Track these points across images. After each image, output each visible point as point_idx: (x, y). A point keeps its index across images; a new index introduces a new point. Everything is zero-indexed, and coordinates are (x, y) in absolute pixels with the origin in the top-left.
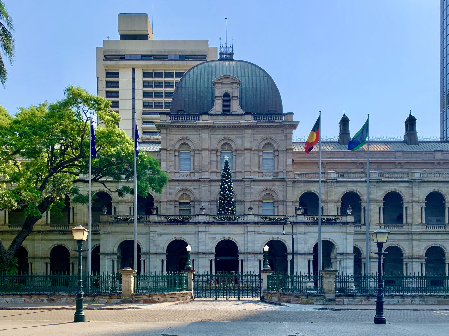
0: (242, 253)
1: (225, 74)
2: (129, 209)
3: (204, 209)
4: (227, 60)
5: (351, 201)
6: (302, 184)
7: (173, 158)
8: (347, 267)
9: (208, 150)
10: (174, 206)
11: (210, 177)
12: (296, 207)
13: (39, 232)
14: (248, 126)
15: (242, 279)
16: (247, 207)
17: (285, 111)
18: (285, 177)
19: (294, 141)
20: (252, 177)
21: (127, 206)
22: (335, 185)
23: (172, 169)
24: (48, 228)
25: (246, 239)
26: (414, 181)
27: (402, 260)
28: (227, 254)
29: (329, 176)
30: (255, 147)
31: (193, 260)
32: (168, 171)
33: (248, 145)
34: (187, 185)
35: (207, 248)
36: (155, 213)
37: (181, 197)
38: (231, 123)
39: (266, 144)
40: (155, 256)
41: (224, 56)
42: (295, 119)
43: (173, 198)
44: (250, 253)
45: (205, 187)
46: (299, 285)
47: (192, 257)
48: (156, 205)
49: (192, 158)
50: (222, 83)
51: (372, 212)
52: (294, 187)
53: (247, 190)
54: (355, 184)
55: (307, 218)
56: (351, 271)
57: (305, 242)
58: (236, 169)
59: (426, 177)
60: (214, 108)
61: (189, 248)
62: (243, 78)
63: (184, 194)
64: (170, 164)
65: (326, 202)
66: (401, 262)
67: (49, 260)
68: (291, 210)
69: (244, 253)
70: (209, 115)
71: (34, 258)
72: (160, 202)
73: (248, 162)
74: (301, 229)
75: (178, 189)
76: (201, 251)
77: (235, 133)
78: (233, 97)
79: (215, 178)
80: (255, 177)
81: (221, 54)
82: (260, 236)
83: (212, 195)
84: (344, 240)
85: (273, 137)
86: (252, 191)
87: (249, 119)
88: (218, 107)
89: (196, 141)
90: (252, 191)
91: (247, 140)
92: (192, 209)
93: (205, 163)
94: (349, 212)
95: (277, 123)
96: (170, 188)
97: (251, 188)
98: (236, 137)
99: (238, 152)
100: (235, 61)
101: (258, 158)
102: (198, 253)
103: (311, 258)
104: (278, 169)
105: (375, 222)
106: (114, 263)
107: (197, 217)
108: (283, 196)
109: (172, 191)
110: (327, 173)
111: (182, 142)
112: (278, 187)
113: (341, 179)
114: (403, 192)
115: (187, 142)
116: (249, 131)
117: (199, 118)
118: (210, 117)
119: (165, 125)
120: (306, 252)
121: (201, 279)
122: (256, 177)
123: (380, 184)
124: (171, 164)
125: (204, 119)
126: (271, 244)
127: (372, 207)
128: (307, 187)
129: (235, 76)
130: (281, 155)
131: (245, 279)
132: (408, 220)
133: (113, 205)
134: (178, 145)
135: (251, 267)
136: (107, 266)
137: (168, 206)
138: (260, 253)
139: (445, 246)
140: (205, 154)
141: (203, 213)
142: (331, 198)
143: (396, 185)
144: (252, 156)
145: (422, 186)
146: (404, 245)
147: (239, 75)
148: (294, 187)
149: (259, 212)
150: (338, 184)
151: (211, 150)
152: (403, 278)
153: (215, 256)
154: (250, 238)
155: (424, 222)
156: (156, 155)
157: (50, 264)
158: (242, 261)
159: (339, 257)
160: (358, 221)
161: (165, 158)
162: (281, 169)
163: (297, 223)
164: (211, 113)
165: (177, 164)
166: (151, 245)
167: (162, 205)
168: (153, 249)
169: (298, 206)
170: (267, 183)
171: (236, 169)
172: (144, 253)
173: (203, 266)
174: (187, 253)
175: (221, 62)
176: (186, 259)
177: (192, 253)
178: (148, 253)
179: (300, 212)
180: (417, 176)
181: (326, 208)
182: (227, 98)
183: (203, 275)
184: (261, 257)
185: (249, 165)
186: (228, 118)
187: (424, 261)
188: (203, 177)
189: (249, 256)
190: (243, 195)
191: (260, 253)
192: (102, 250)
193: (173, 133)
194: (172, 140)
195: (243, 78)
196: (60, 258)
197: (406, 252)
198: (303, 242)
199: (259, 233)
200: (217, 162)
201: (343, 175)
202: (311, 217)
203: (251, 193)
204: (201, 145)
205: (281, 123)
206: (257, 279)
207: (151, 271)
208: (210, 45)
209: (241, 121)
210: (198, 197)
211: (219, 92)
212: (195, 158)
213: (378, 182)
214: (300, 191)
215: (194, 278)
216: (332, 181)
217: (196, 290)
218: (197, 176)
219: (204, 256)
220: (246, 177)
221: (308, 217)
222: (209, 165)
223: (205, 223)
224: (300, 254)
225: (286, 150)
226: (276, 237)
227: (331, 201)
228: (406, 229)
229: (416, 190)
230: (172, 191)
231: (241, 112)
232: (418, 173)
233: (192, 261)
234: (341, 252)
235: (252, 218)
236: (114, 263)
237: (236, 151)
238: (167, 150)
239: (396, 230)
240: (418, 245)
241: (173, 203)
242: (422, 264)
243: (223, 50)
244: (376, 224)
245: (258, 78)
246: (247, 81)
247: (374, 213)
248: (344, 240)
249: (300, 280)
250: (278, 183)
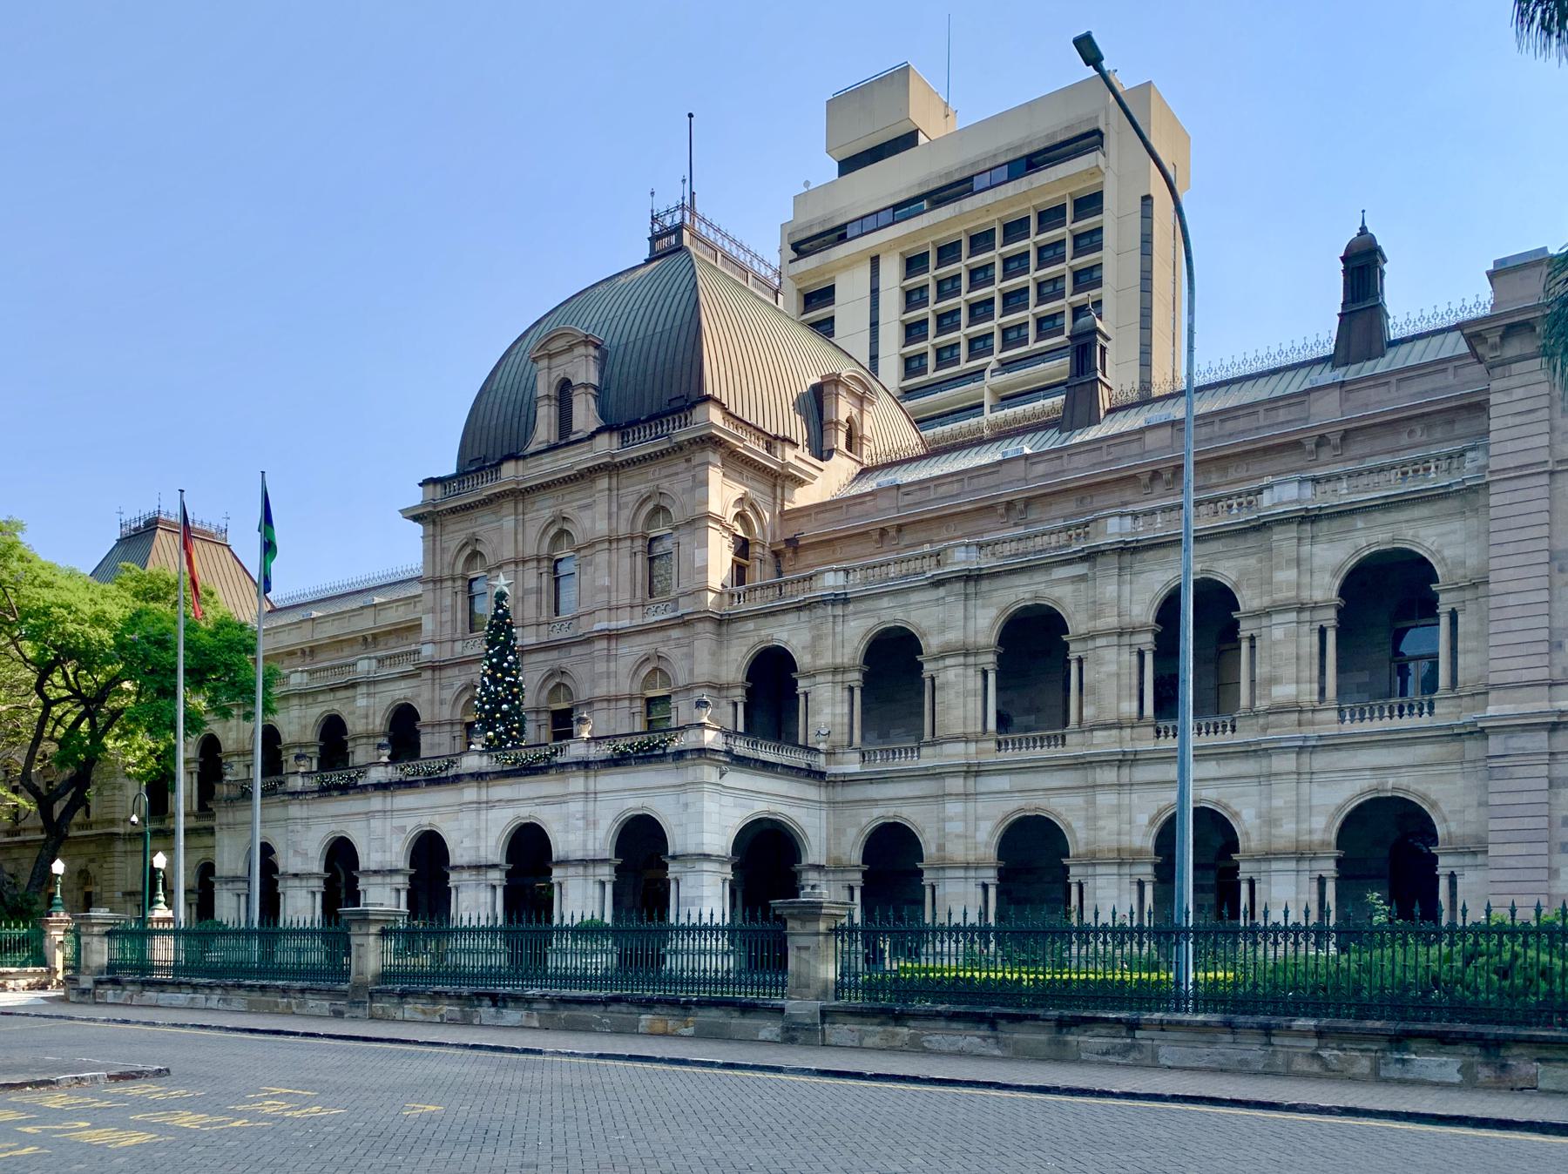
6: (751, 625)
9: (516, 563)
22: (839, 611)
23: (448, 630)
33: (602, 528)
38: (554, 473)
54: (901, 600)
77: (578, 495)
96: (442, 688)
98: (580, 507)
99: (583, 553)
112: (678, 646)
118: (521, 463)
122: (624, 622)
123: (985, 585)
127: (951, 675)
139: (1235, 805)
143: (1039, 577)
145: (1137, 567)
150: (851, 607)
170: (652, 637)
193: (451, 528)
214: (745, 650)
216: (823, 602)
227: (822, 671)
228: (1075, 745)
229: (1109, 589)
238: (434, 582)
239: (1039, 752)
241: (448, 728)
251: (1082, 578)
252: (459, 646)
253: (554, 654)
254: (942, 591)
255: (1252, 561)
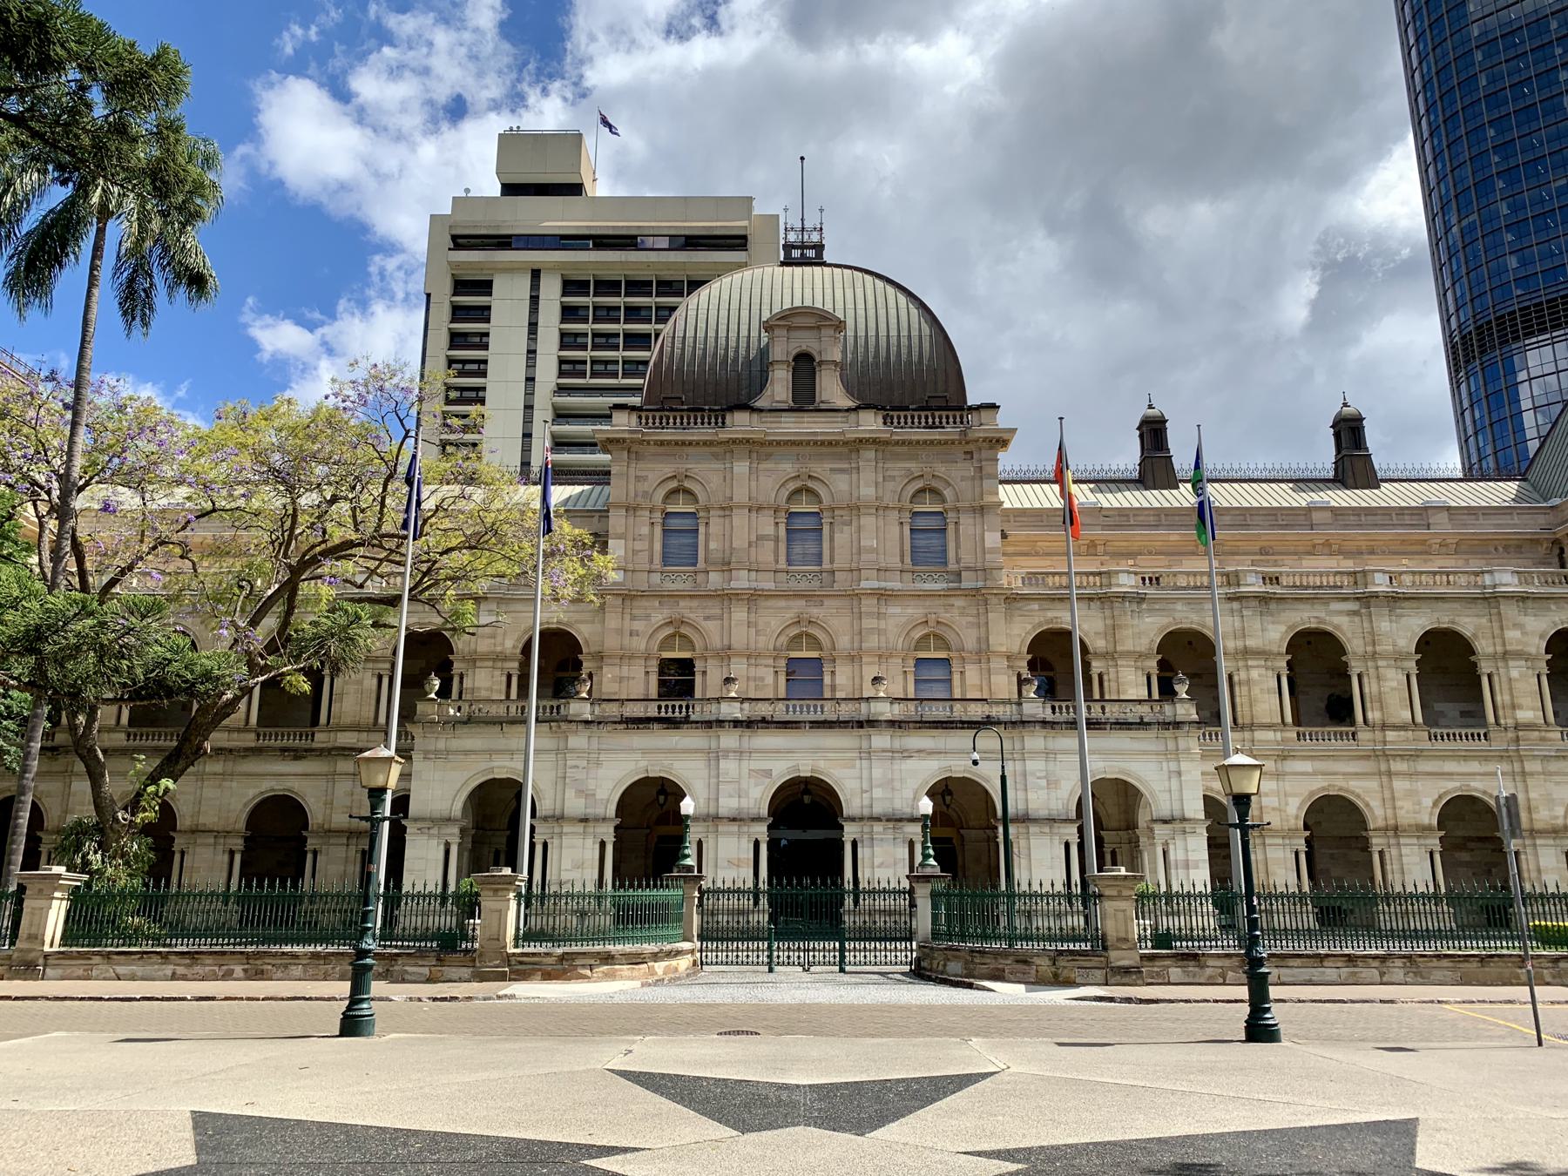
0: (852, 819)
1: (797, 303)
2: (504, 678)
3: (734, 680)
4: (804, 262)
5: (1186, 662)
7: (645, 530)
8: (1189, 865)
10: (643, 670)
11: (754, 585)
12: (1019, 675)
13: (218, 751)
14: (867, 440)
15: (856, 902)
16: (870, 672)
17: (972, 399)
18: (980, 584)
19: (1003, 476)
20: (883, 584)
21: (497, 673)
24: (249, 740)
25: (865, 774)
26: (1375, 595)
27: (1366, 839)
28: (806, 826)
29: (1114, 581)
30: (889, 499)
31: (700, 844)
32: (630, 567)
33: (867, 492)
34: (686, 609)
35: (744, 803)
36: (584, 695)
37: (666, 643)
39: (922, 491)
40: (580, 828)
41: (796, 253)
42: (1002, 420)
43: (640, 644)
44: (878, 819)
45: (739, 614)
46: (1039, 922)
47: (694, 833)
48: (587, 666)
49: (702, 529)
50: (789, 328)
51: (1256, 691)
52: (1009, 617)
53: (868, 623)
55: (1053, 708)
56: (1200, 877)
57: (1052, 783)
58: (832, 562)
59: (1407, 585)
60: (768, 392)
61: (687, 806)
62: (850, 313)
63: (673, 636)
64: (637, 548)
65: (1110, 656)
66: (1365, 846)
67: (241, 841)
68: (1004, 685)
69: (861, 819)
70: (753, 410)
71: (195, 831)
72: (600, 657)
73: (869, 541)
74: (1035, 740)
75: (659, 617)
76: (723, 812)
78: (821, 363)
79: (772, 585)
80: (889, 585)
81: (788, 247)
82: (910, 764)
83: (762, 639)
84: (1174, 779)
85: (941, 469)
86: (883, 624)
87: (871, 423)
88: (780, 386)
89: (715, 481)
90: (883, 624)
91: (865, 481)
92: (698, 679)
93: (740, 542)
94: (1182, 690)
95: (951, 431)
96: (633, 618)
97: (879, 616)
100: (830, 265)
101: (897, 529)
102: (714, 819)
103: (1071, 832)
104: (958, 562)
105: (1267, 720)
106: (447, 853)
107: (714, 707)
108: (979, 639)
109: (638, 625)
110: (1108, 573)
111: (674, 484)
112: (962, 614)
113: (1151, 591)
114: (1345, 628)
115: (687, 484)
116: (869, 454)
117: (724, 418)
118: (755, 416)
119: (624, 440)
120: (1054, 814)
121: (724, 902)
123: (1273, 606)
124: (639, 545)
125: (740, 423)
126: (942, 791)
127: (1255, 674)
128: (1050, 614)
129: (829, 307)
130: (966, 521)
131: (866, 902)
132: (1370, 715)
133: (457, 667)
134: (661, 493)
135: (882, 863)
136: (426, 864)
137: (625, 671)
138: (913, 820)
140: (740, 519)
141: (733, 694)
142: (1127, 645)
144: (881, 523)
146: (1366, 792)
147: (840, 305)
148: (1009, 617)
149: (905, 690)
151: (759, 509)
152: (1373, 900)
153: (770, 827)
154: (877, 772)
155: (1419, 718)
156: (596, 519)
157: (243, 853)
158: (854, 844)
159: (1160, 830)
160: (1211, 717)
161: (621, 530)
162: (967, 559)
163: (1023, 722)
164: (760, 403)
165: (658, 546)
166: (570, 794)
167: (605, 669)
168: (574, 805)
169: (1026, 674)
171: (832, 562)
172: (545, 819)
173: (730, 860)
174: (681, 821)
175: (788, 270)
176: (680, 840)
177: (696, 819)
178: (559, 818)
179: (1030, 691)
180: (1380, 584)
181: (1112, 676)
182: (805, 365)
183: (729, 891)
184: (915, 830)
185: (872, 550)
186: (807, 417)
187: (1434, 843)
188: (733, 584)
189: (878, 827)
190: (857, 638)
191: (913, 820)
192: (414, 808)
194: (645, 478)
195: (850, 313)
196: (277, 835)
197: (1377, 814)
198: (1043, 783)
199: (906, 754)
200: (777, 540)
201: (1155, 580)
202: (1064, 705)
203: (880, 632)
204: (728, 494)
205: (964, 433)
206: (903, 903)
207: (565, 876)
208: (759, 209)
209: (845, 427)
210: (716, 642)
211: (782, 350)
212: (712, 529)
213: (1264, 599)
215: (701, 899)
216: (1123, 597)
217: (707, 939)
218: (715, 580)
219: (734, 828)
220: (864, 584)
221: (1057, 704)
222: (753, 549)
223: (737, 723)
224: (1036, 821)
225: (982, 508)
226: (959, 767)
229: (1384, 625)
230: (638, 625)
231: (849, 403)
232: (1384, 572)
233: (695, 847)
234: (1166, 813)
235: (885, 711)
236: (447, 853)
237: (833, 509)
240: (1410, 794)
242: (1431, 854)
243: (792, 237)
244: (1269, 727)
245: (893, 312)
246: (861, 321)
247: (1261, 691)
248: (1174, 779)
249: (1042, 905)
250: (959, 602)
251: (1355, 613)
252: (656, 578)
253: (803, 602)
254: (1236, 605)
255: (1484, 621)
